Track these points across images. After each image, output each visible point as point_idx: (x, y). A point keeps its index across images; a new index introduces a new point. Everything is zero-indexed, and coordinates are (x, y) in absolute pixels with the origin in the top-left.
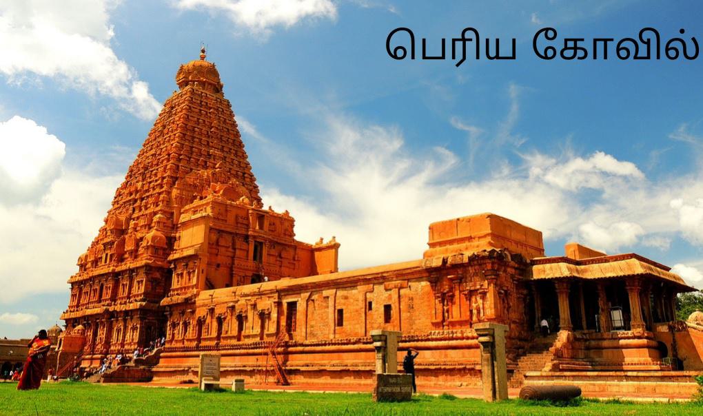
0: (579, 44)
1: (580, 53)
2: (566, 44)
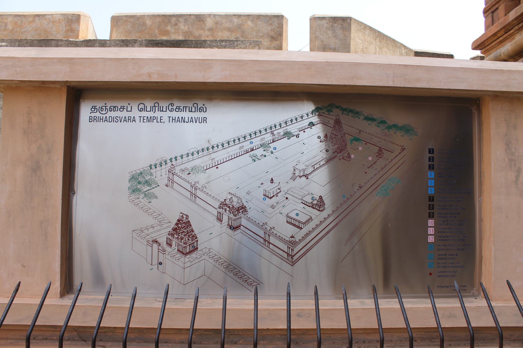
0: (180, 108)
1: (180, 110)
2: (177, 107)
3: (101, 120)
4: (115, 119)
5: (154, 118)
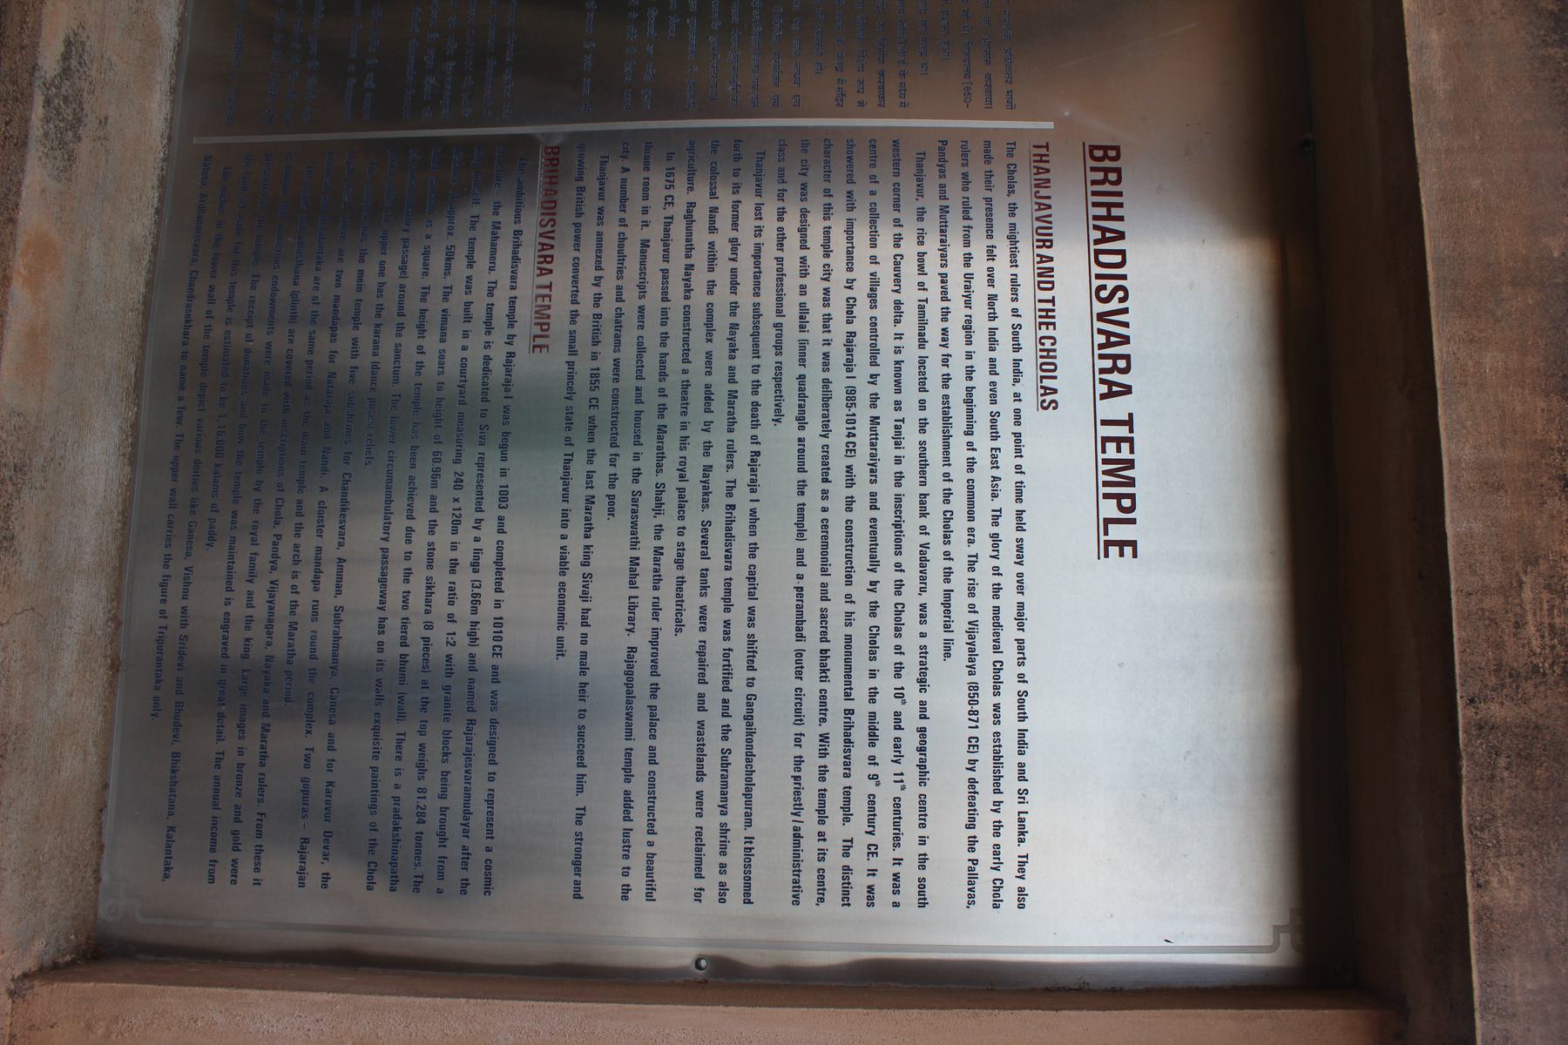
3: (1102, 211)
4: (1111, 284)
5: (1126, 503)
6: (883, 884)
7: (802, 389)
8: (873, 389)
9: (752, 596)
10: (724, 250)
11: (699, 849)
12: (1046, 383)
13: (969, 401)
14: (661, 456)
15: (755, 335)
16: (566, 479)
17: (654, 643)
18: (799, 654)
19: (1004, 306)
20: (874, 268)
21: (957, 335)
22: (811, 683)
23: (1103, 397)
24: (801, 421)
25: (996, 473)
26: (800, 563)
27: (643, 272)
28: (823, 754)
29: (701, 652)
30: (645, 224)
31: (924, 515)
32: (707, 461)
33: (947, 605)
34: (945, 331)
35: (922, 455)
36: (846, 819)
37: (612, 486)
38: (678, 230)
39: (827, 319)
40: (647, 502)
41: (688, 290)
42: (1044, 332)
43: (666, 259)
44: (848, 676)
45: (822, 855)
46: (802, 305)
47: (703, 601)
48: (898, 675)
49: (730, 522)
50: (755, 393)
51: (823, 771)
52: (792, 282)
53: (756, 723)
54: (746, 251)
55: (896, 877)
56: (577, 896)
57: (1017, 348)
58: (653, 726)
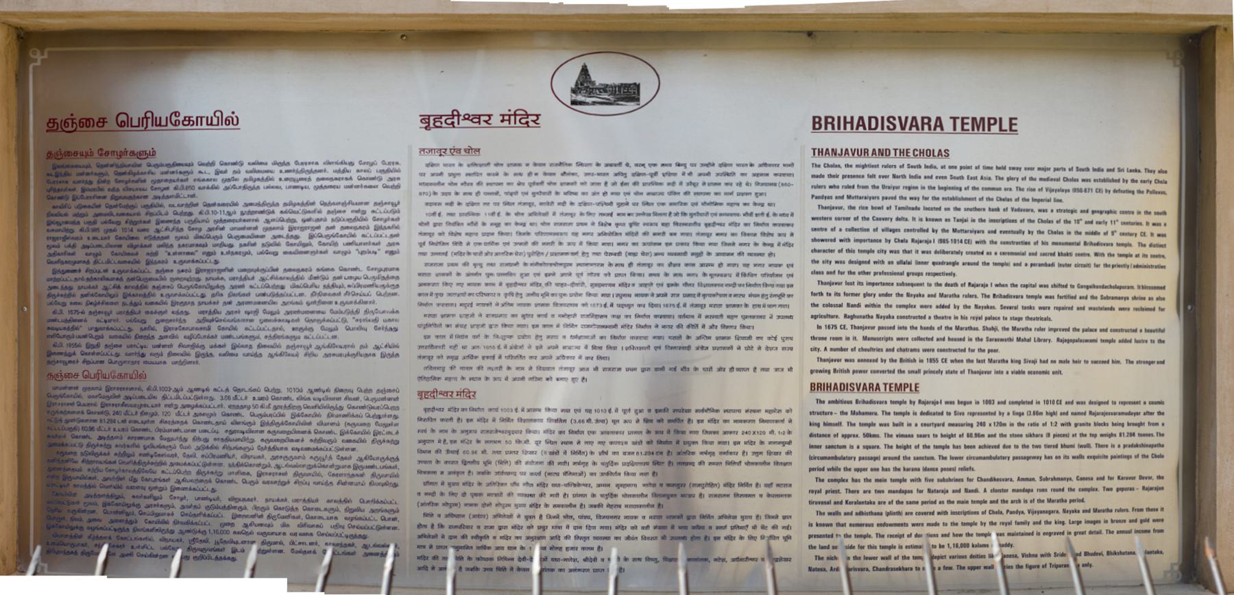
3: (849, 126)
4: (886, 123)
5: (992, 121)
6: (1157, 230)
7: (940, 263)
8: (939, 231)
9: (1034, 286)
10: (869, 300)
11: (1142, 309)
12: (936, 154)
13: (945, 189)
14: (970, 328)
15: (912, 285)
16: (980, 373)
17: (1055, 330)
18: (1060, 265)
19: (898, 172)
20: (880, 230)
21: (913, 193)
22: (1072, 260)
23: (942, 129)
24: (954, 264)
25: (979, 178)
26: (1020, 265)
27: (879, 339)
28: (1103, 255)
29: (1059, 309)
30: (855, 338)
31: (998, 210)
32: (973, 306)
33: (1039, 201)
34: (911, 198)
35: (971, 210)
36: (1130, 245)
37: (984, 351)
38: (857, 322)
39: (905, 251)
40: (992, 334)
41: (889, 317)
42: (911, 154)
43: (873, 328)
44: (1070, 244)
45: (1145, 256)
46: (898, 263)
47: (1037, 308)
48: (1070, 222)
49: (1001, 296)
50: (940, 285)
51: (1110, 255)
52: (886, 268)
53: (1089, 284)
54: (870, 290)
55: (1154, 224)
56: (1163, 362)
57: (920, 167)
58: (1091, 330)
